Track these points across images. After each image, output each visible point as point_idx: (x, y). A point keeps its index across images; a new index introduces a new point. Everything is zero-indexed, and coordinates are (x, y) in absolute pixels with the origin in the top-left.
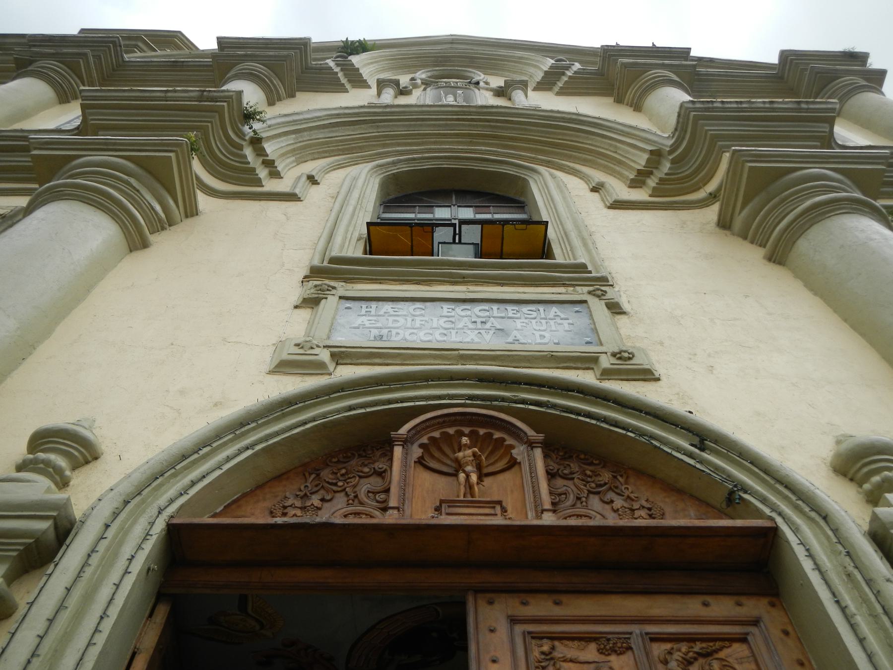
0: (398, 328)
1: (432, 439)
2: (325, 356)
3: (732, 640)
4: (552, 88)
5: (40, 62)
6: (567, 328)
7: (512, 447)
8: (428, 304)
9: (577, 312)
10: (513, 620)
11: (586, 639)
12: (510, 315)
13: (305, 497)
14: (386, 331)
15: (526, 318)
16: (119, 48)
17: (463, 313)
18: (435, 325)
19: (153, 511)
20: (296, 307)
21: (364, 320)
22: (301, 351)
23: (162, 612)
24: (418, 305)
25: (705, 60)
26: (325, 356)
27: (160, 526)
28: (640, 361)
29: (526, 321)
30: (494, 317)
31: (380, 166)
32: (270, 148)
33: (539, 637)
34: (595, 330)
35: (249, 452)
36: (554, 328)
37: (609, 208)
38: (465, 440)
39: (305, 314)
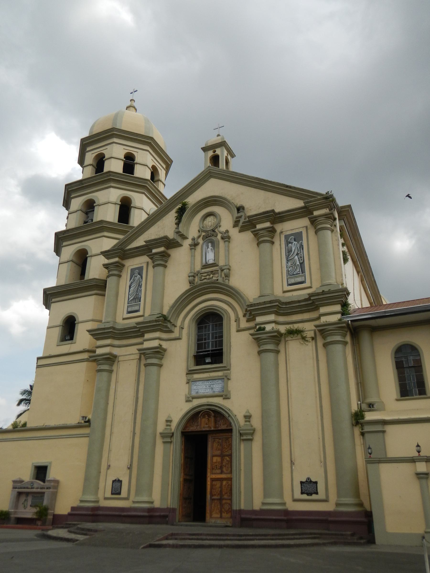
0: (199, 389)
1: (203, 415)
2: (191, 399)
3: (229, 438)
4: (239, 224)
5: (110, 267)
6: (221, 387)
7: (211, 416)
8: (203, 381)
9: (223, 381)
10: (212, 437)
11: (217, 438)
12: (214, 383)
13: (192, 423)
14: (198, 390)
15: (216, 384)
16: (122, 249)
17: (208, 384)
18: (204, 388)
19: (179, 431)
20: (186, 384)
21: (195, 387)
22: (188, 399)
23: (184, 436)
24: (202, 382)
25: (289, 187)
26: (191, 399)
27: (180, 432)
28: (228, 396)
29: (215, 385)
30: (212, 384)
31: (194, 318)
32: (172, 321)
33: (215, 438)
34: (224, 387)
35: (186, 421)
36: (219, 387)
37: (237, 332)
38: (206, 416)
39: (187, 385)
